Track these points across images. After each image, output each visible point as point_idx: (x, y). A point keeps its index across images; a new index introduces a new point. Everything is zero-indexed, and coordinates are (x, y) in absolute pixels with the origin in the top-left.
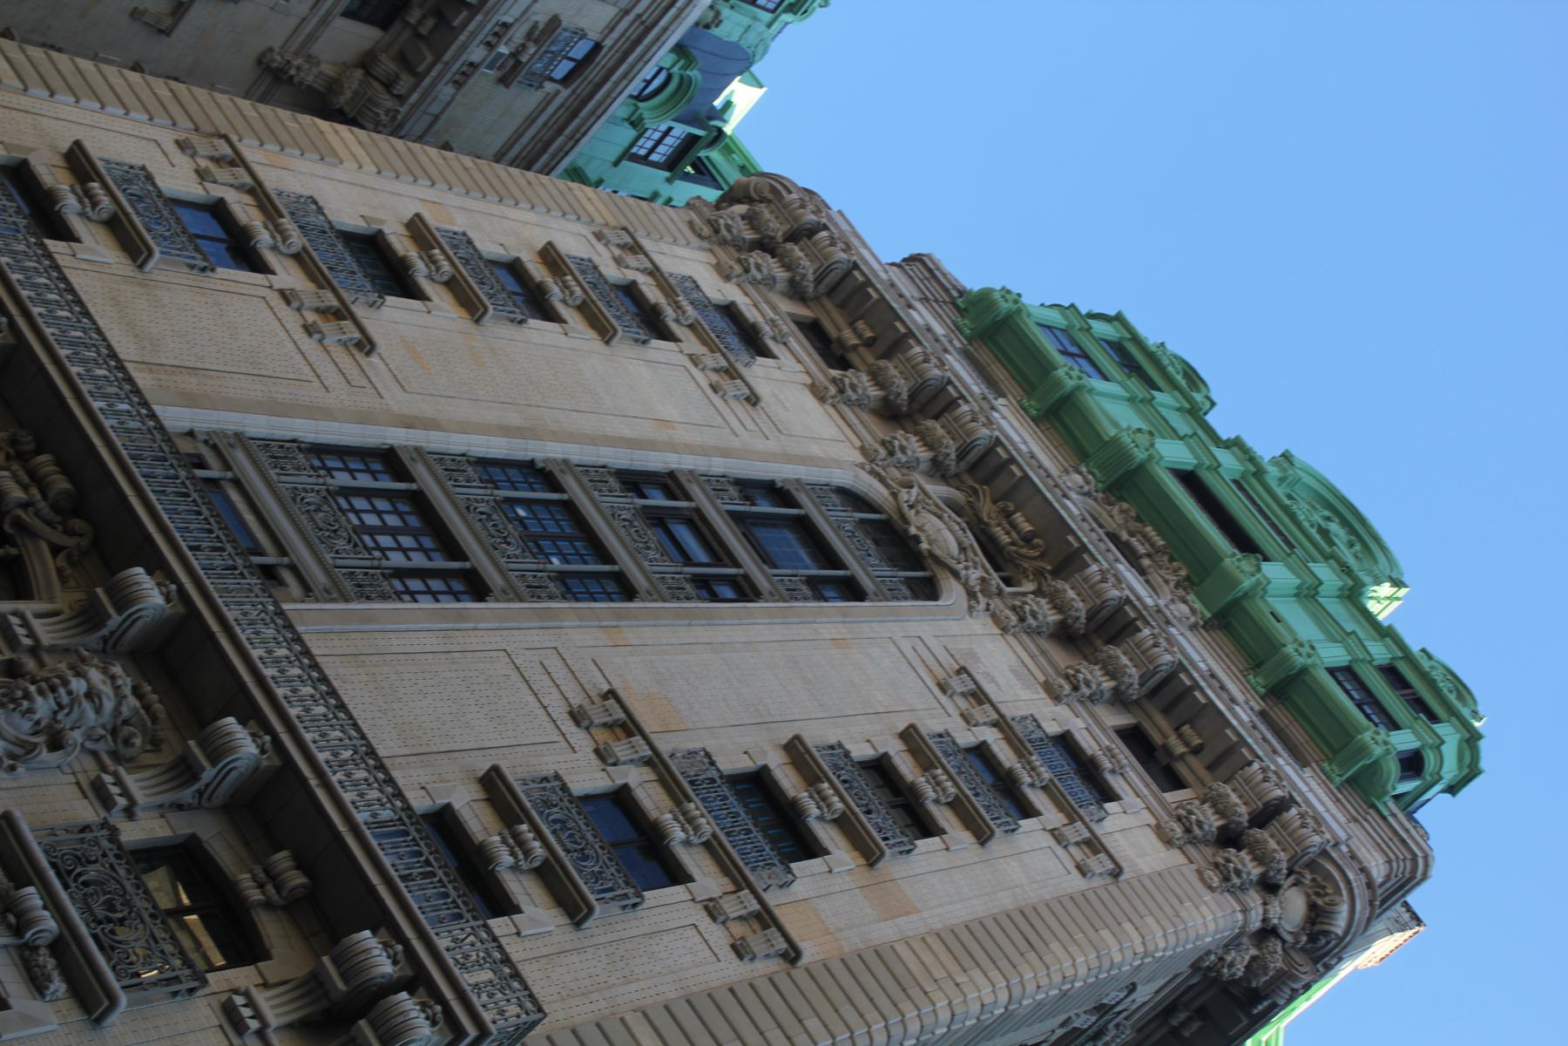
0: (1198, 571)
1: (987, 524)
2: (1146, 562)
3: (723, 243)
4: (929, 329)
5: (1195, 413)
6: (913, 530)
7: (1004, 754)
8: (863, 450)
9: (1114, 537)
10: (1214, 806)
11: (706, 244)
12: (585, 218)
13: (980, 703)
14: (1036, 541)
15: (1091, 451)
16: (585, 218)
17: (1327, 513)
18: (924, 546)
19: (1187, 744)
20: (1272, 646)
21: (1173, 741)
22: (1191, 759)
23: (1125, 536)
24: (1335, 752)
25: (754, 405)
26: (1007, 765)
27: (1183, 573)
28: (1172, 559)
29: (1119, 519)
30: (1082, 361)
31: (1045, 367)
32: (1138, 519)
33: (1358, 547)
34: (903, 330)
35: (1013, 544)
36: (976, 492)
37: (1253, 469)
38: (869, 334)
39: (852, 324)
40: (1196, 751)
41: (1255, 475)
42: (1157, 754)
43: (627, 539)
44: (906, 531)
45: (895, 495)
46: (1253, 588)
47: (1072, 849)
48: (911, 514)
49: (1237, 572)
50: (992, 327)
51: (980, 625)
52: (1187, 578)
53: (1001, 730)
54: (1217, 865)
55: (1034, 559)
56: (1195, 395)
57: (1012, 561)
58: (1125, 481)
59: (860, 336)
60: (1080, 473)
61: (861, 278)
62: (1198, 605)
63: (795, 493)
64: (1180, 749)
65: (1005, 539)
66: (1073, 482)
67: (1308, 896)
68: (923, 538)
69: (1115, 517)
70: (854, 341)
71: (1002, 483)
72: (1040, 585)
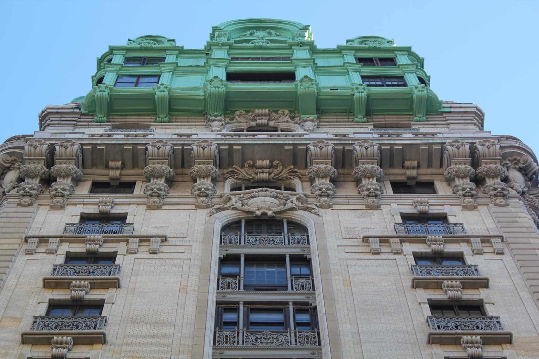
0: (293, 105)
1: (252, 179)
2: (272, 123)
3: (37, 197)
4: (93, 136)
5: (181, 51)
6: (259, 213)
7: (78, 248)
8: (198, 207)
9: (250, 129)
10: (154, 177)
11: (36, 205)
12: (15, 253)
13: (47, 242)
14: (274, 163)
15: (201, 108)
16: (15, 253)
17: (249, 32)
18: (270, 213)
19: (413, 168)
20: (350, 100)
21: (410, 173)
22: (421, 171)
23: (253, 124)
24: (411, 109)
25: (166, 240)
26: (84, 250)
27: (287, 112)
28: (276, 112)
29: (242, 120)
30: (142, 80)
31: (150, 99)
32: (247, 112)
33: (273, 32)
34: (130, 147)
35: (270, 174)
36: (233, 172)
37: (228, 47)
38: (119, 164)
39: (107, 167)
40: (418, 167)
41: (230, 49)
42: (408, 184)
43: (270, 345)
44: (257, 216)
45: (235, 209)
46: (317, 89)
47: (39, 250)
48: (246, 208)
49: (308, 90)
50: (105, 107)
51: (327, 215)
52: (291, 112)
53: (405, 242)
54: (495, 196)
55: (282, 170)
56: (161, 45)
57: (278, 180)
58: (228, 106)
59: (117, 168)
60: (214, 121)
61: (89, 147)
62: (312, 117)
63: (228, 252)
64: (414, 173)
65: (265, 176)
66: (216, 127)
67: (515, 168)
68: (267, 211)
69: (241, 121)
70: (118, 173)
71: (237, 158)
72: (298, 176)
